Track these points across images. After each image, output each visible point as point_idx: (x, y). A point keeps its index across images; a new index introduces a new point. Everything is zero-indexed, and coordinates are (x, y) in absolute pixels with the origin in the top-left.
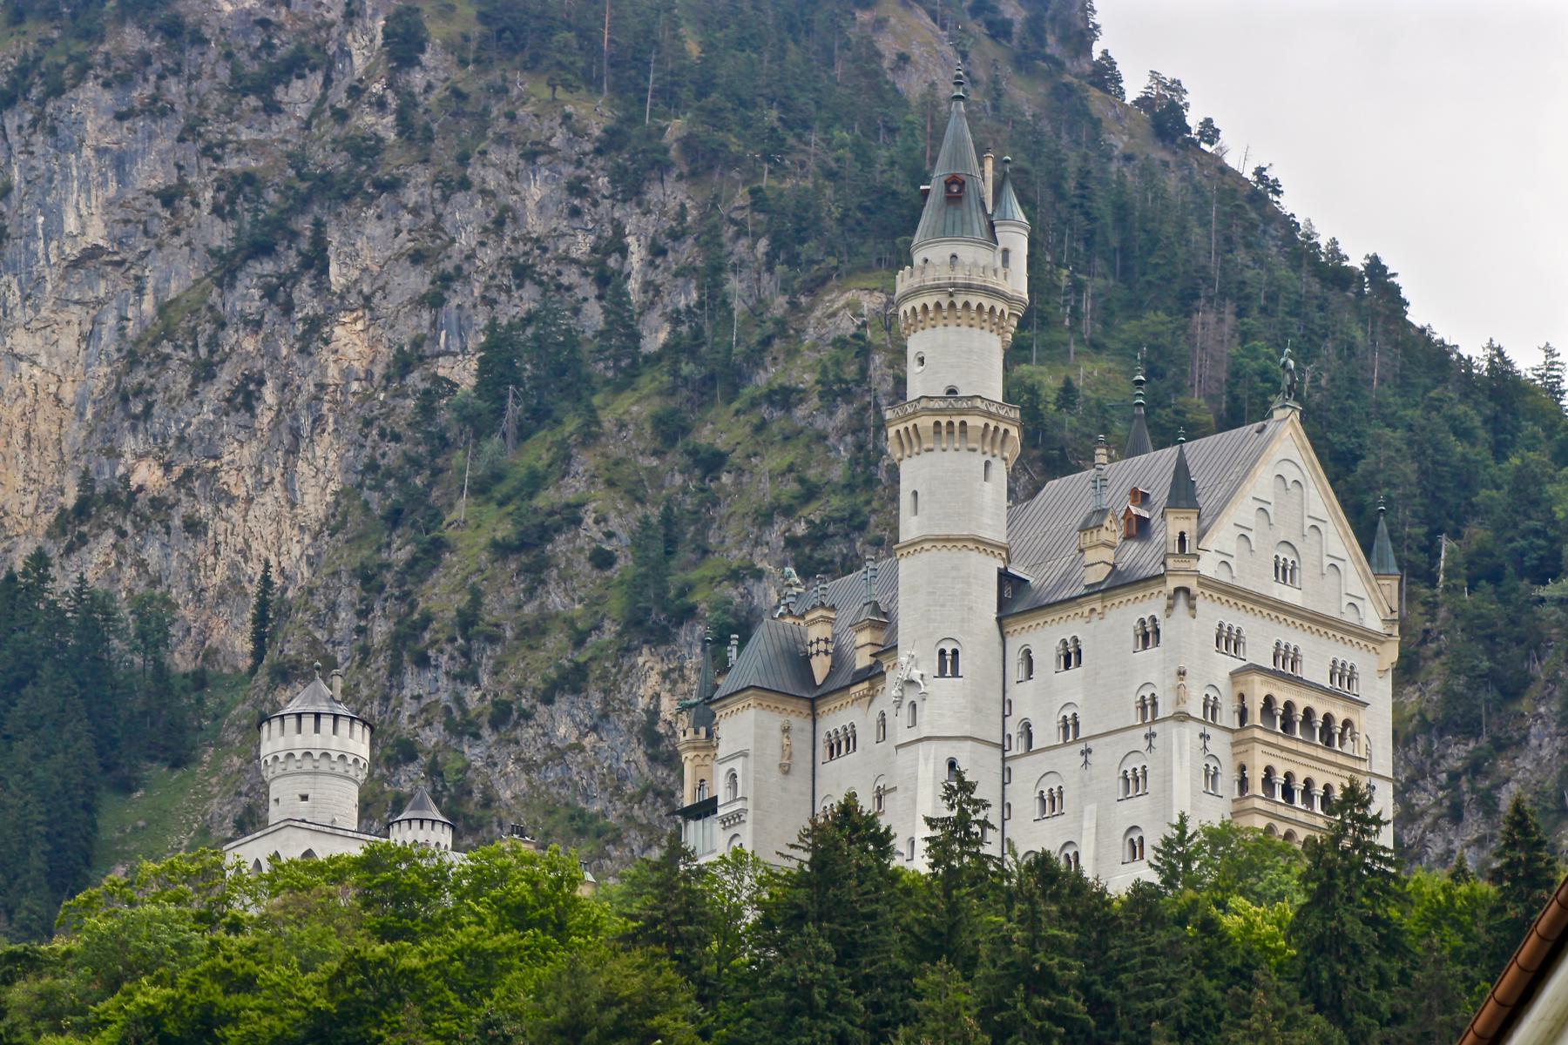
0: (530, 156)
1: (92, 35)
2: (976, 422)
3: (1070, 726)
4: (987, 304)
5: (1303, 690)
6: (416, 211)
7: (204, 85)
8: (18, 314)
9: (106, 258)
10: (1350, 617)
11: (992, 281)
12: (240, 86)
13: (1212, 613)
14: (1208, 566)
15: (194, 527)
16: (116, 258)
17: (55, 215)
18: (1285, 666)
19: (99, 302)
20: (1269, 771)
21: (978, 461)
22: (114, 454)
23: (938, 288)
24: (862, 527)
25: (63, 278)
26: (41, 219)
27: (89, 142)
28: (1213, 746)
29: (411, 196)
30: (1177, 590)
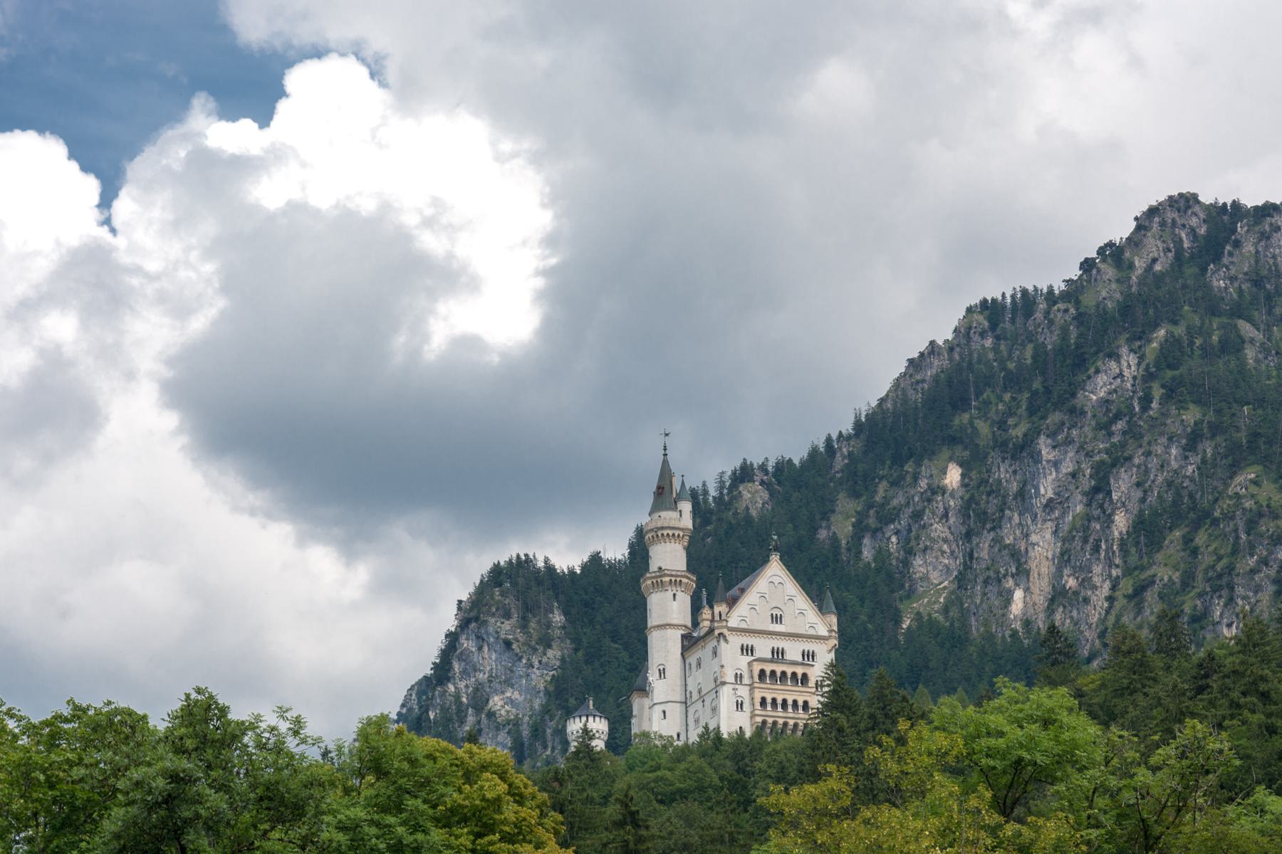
0: (1170, 439)
1: (1044, 418)
2: (667, 579)
3: (700, 691)
4: (671, 533)
6: (1139, 467)
7: (1086, 429)
10: (812, 632)
11: (673, 524)
12: (1099, 427)
13: (736, 641)
14: (733, 622)
15: (1086, 600)
17: (1037, 488)
18: (778, 655)
21: (670, 594)
22: (1062, 577)
24: (1233, 569)
28: (739, 693)
29: (1136, 461)
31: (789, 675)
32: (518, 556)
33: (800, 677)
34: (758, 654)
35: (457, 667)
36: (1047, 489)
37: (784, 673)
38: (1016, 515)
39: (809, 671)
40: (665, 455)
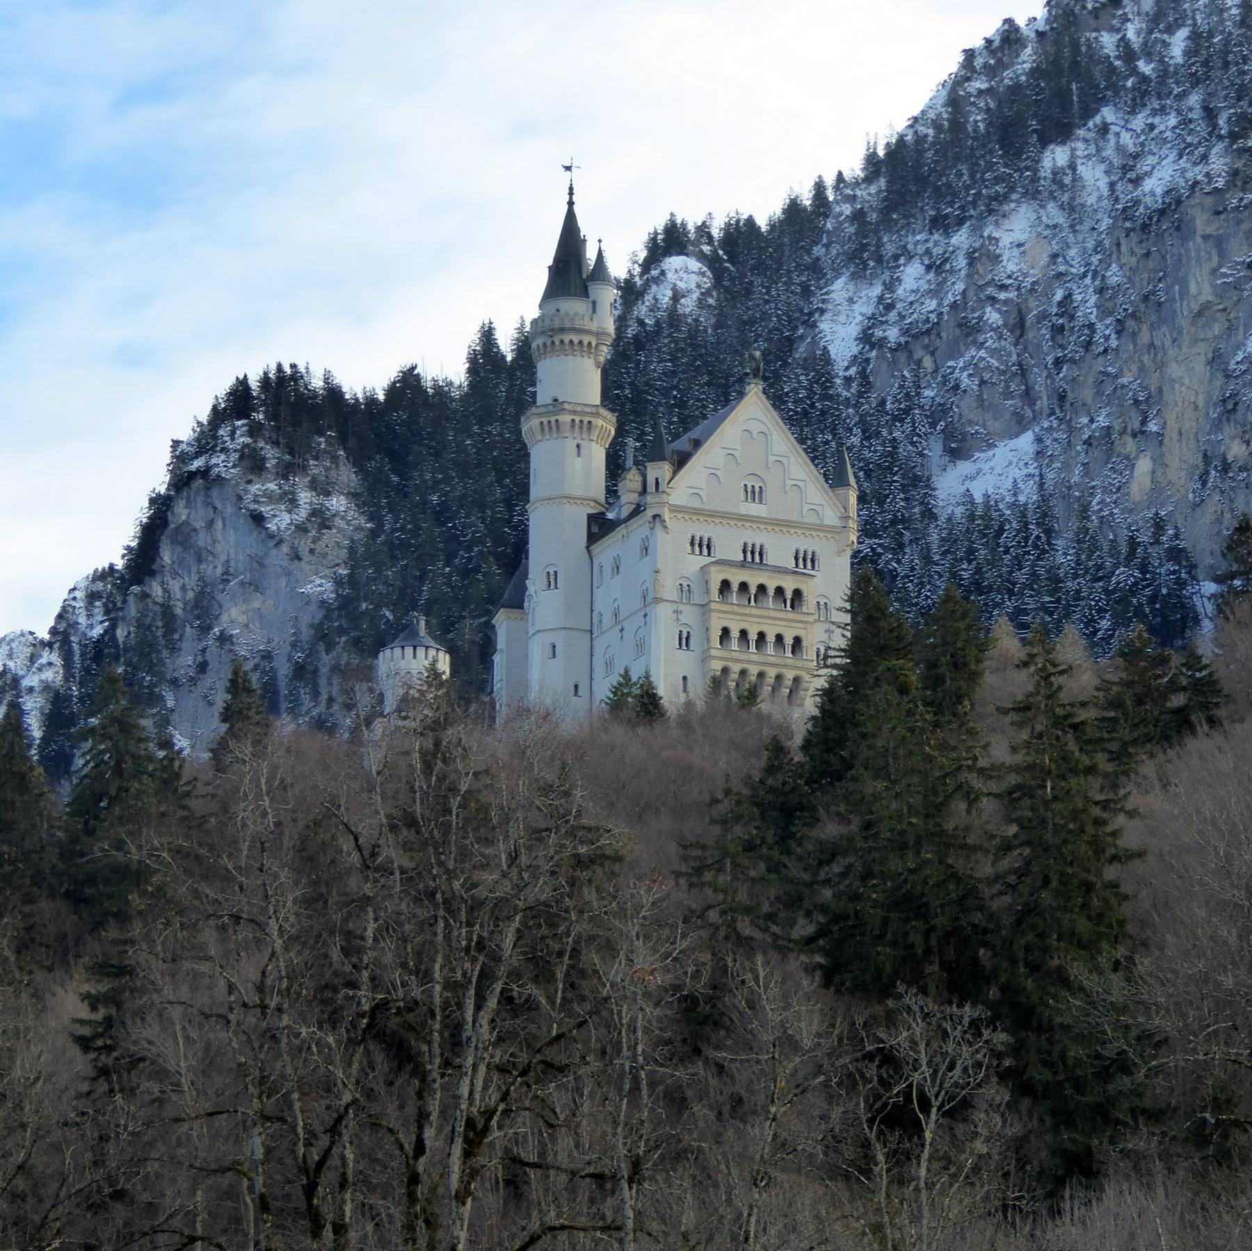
2: (566, 418)
4: (576, 339)
5: (754, 572)
8: (1170, 352)
9: (1215, 308)
10: (811, 519)
16: (1221, 307)
18: (754, 556)
19: (1216, 337)
20: (726, 632)
21: (570, 444)
23: (543, 333)
25: (1192, 325)
26: (1177, 287)
27: (1199, 232)
30: (654, 517)
31: (771, 592)
32: (280, 368)
33: (789, 595)
34: (718, 554)
35: (167, 555)
36: (1200, 287)
37: (762, 588)
38: (1145, 328)
39: (807, 587)
40: (571, 203)
